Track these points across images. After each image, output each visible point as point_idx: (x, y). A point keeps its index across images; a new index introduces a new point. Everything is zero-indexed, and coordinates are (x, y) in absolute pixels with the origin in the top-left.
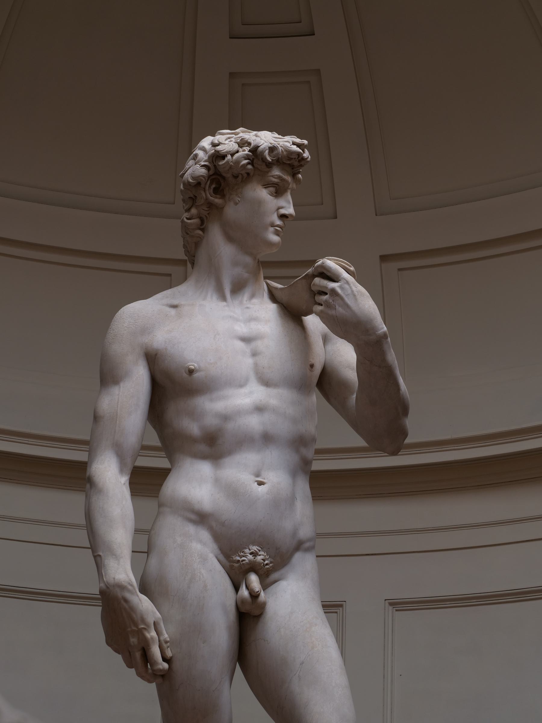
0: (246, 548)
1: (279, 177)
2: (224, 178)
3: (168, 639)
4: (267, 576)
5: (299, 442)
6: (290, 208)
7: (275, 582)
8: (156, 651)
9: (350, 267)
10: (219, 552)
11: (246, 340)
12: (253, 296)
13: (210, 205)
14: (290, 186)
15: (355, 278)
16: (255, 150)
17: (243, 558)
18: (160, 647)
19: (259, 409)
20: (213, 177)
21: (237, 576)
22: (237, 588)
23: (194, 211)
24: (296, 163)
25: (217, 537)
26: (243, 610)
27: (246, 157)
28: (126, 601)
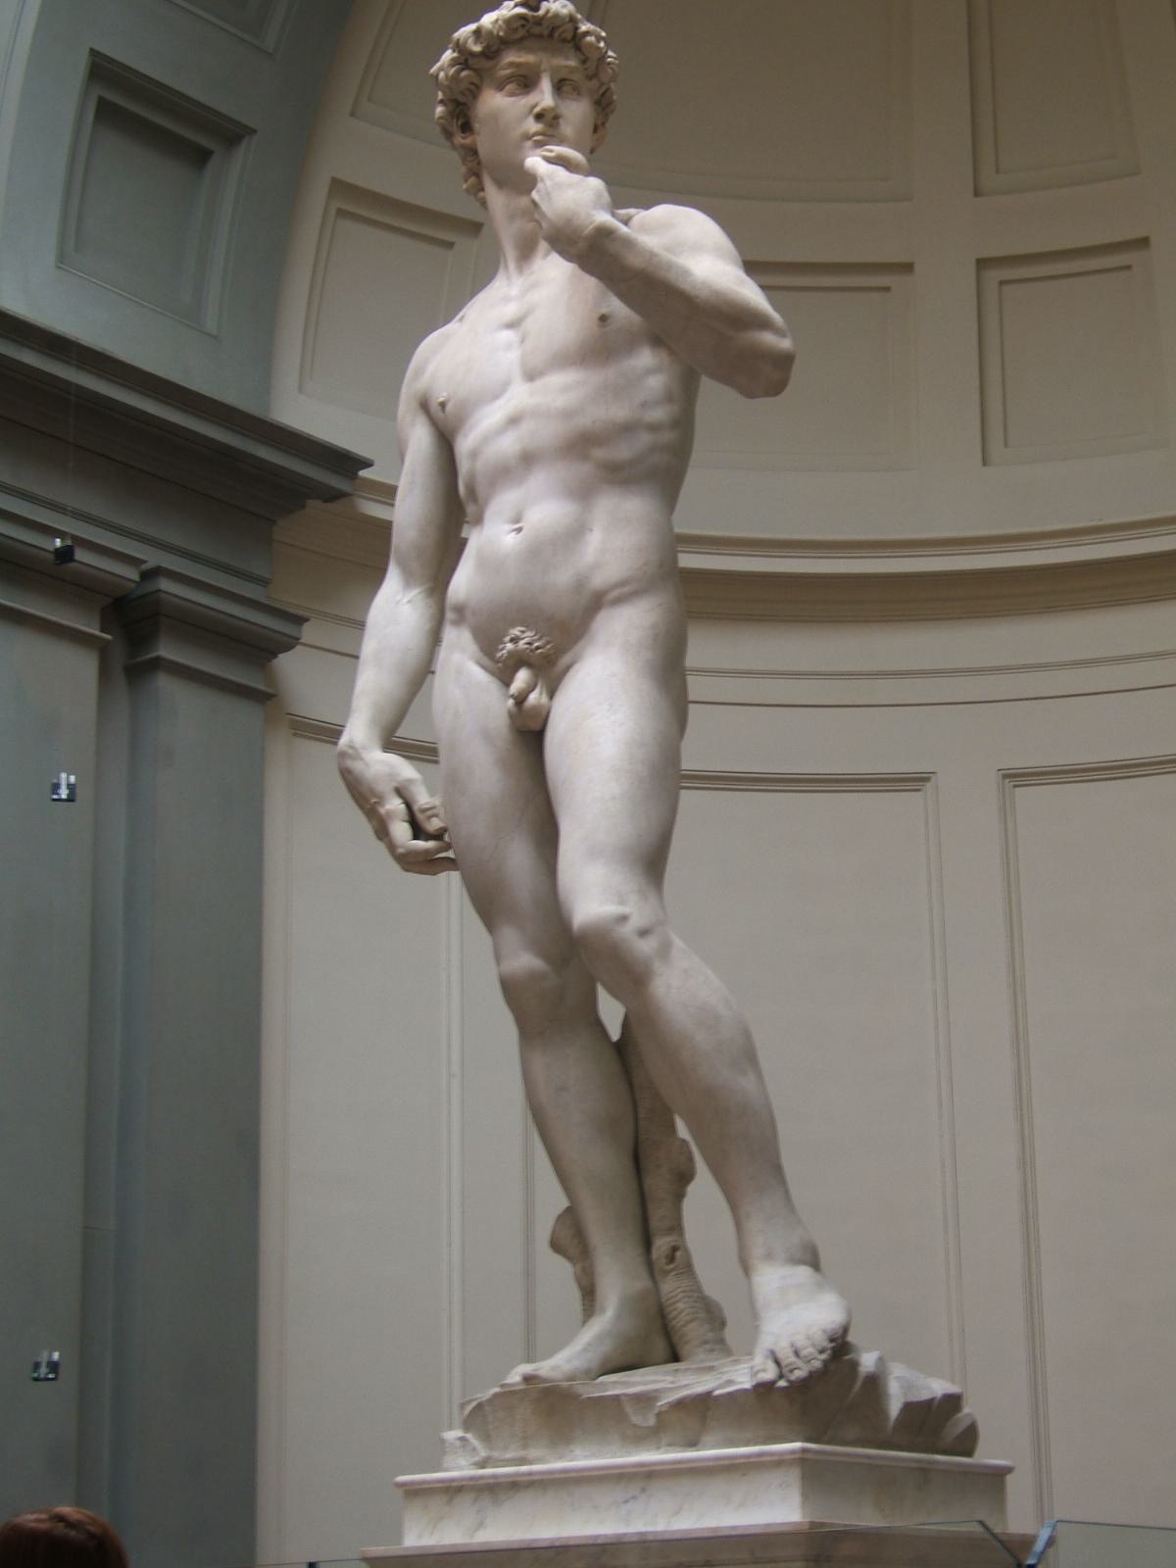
0: (505, 636)
1: (511, 65)
2: (464, 104)
5: (580, 444)
6: (542, 100)
7: (568, 668)
9: (551, 151)
10: (479, 655)
11: (513, 325)
16: (459, 47)
17: (504, 651)
19: (514, 421)
20: (458, 110)
21: (505, 678)
24: (536, 30)
27: (454, 62)
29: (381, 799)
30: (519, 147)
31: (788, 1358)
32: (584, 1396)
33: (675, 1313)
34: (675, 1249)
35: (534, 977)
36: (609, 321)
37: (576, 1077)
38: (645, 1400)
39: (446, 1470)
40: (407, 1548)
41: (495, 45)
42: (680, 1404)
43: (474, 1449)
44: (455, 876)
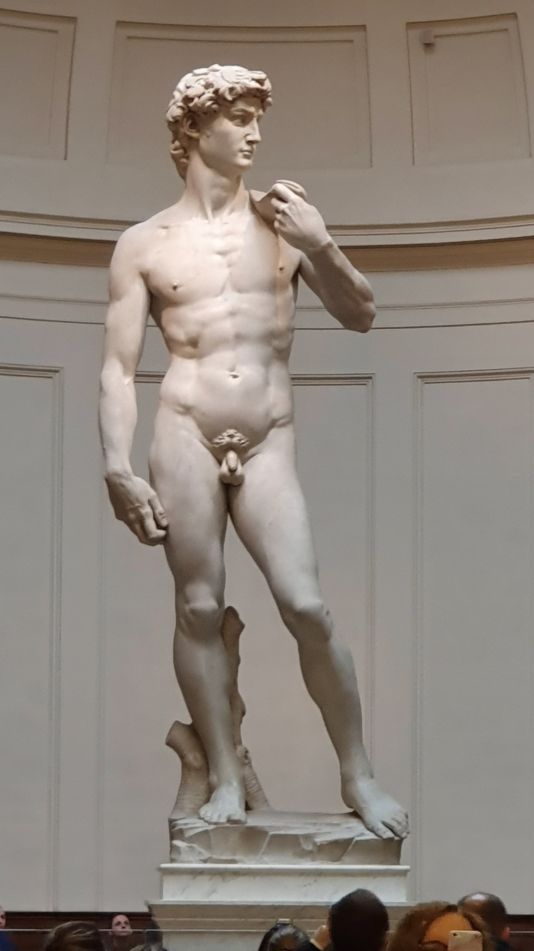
0: (224, 432)
1: (243, 110)
2: (198, 115)
3: (162, 512)
4: (243, 453)
5: (270, 336)
8: (150, 524)
10: (202, 437)
11: (222, 253)
12: (232, 211)
13: (190, 138)
14: (256, 114)
16: (216, 92)
17: (222, 441)
18: (155, 519)
19: (232, 314)
21: (219, 453)
22: (220, 463)
23: (177, 143)
24: (259, 95)
25: (201, 425)
26: (225, 481)
27: (211, 99)
28: (123, 486)
29: (142, 505)
30: (235, 155)
31: (398, 828)
33: (251, 785)
34: (247, 752)
35: (214, 612)
36: (283, 271)
37: (206, 660)
38: (308, 837)
39: (182, 862)
40: (165, 901)
42: (335, 843)
43: (200, 853)
44: (160, 548)
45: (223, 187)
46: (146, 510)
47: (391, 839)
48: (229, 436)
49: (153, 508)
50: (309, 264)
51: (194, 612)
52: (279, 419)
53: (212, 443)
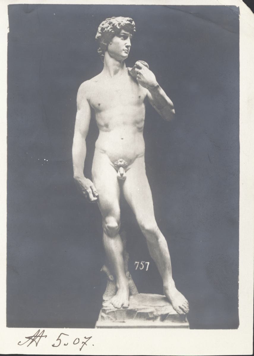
1: (124, 33)
8: (91, 196)
14: (129, 35)
15: (148, 68)
16: (113, 25)
21: (117, 168)
25: (110, 158)
27: (111, 28)
28: (80, 181)
32: (138, 312)
36: (141, 97)
41: (123, 28)
45: (117, 65)
46: (89, 190)
47: (183, 314)
48: (120, 161)
49: (92, 189)
50: (150, 95)
51: (108, 227)
52: (139, 155)
53: (114, 164)
